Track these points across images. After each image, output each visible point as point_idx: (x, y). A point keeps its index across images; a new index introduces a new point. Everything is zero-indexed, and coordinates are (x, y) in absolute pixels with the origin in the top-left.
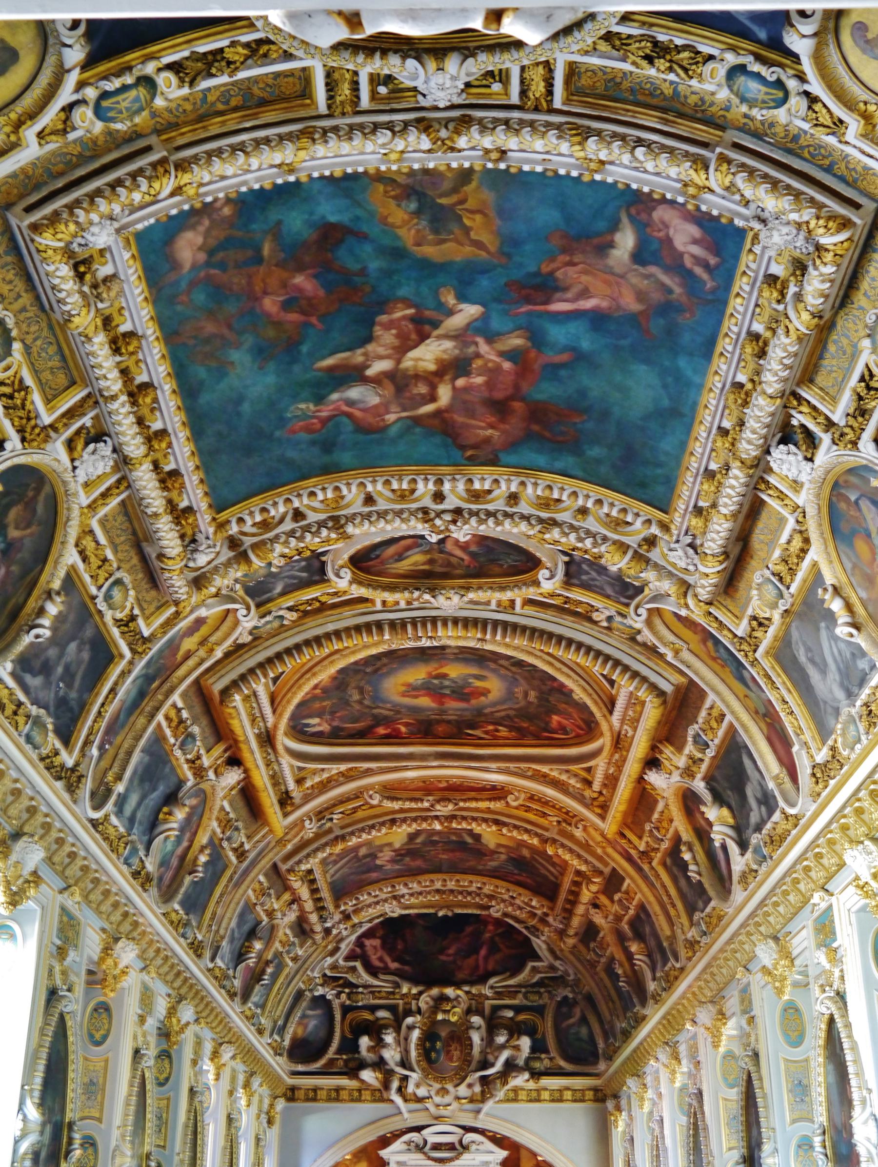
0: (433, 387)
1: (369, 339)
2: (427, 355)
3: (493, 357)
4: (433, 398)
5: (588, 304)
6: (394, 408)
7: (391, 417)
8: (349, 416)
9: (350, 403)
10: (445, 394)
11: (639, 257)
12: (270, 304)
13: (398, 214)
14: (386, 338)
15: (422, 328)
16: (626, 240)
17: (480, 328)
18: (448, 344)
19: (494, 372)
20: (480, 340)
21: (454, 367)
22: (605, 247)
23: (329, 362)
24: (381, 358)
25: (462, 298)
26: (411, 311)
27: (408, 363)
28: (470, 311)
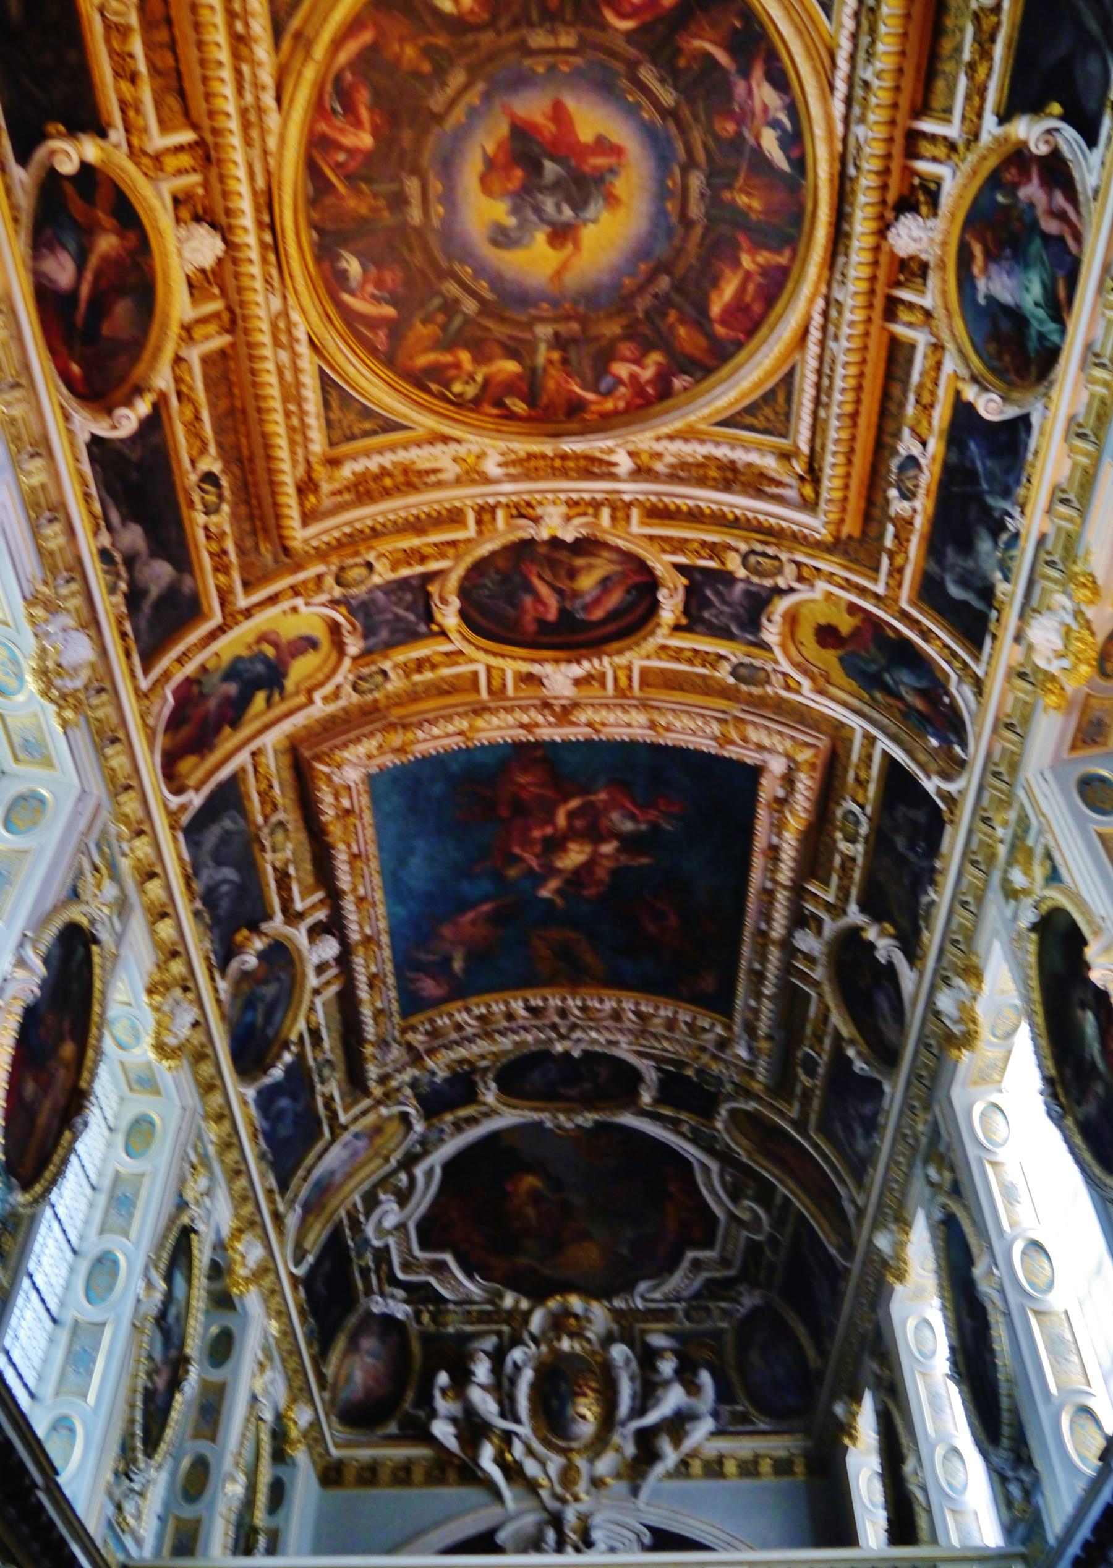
0: (570, 826)
1: (614, 873)
2: (574, 856)
3: (526, 855)
4: (571, 815)
5: (470, 916)
6: (600, 805)
7: (603, 796)
8: (635, 803)
9: (632, 817)
10: (561, 820)
11: (448, 960)
12: (673, 921)
13: (589, 958)
14: (601, 873)
15: (578, 878)
16: (457, 965)
17: (538, 879)
18: (560, 864)
19: (526, 843)
20: (536, 868)
21: (555, 845)
22: (468, 959)
23: (645, 861)
24: (606, 856)
25: (548, 902)
26: (585, 893)
27: (588, 849)
28: (545, 893)
